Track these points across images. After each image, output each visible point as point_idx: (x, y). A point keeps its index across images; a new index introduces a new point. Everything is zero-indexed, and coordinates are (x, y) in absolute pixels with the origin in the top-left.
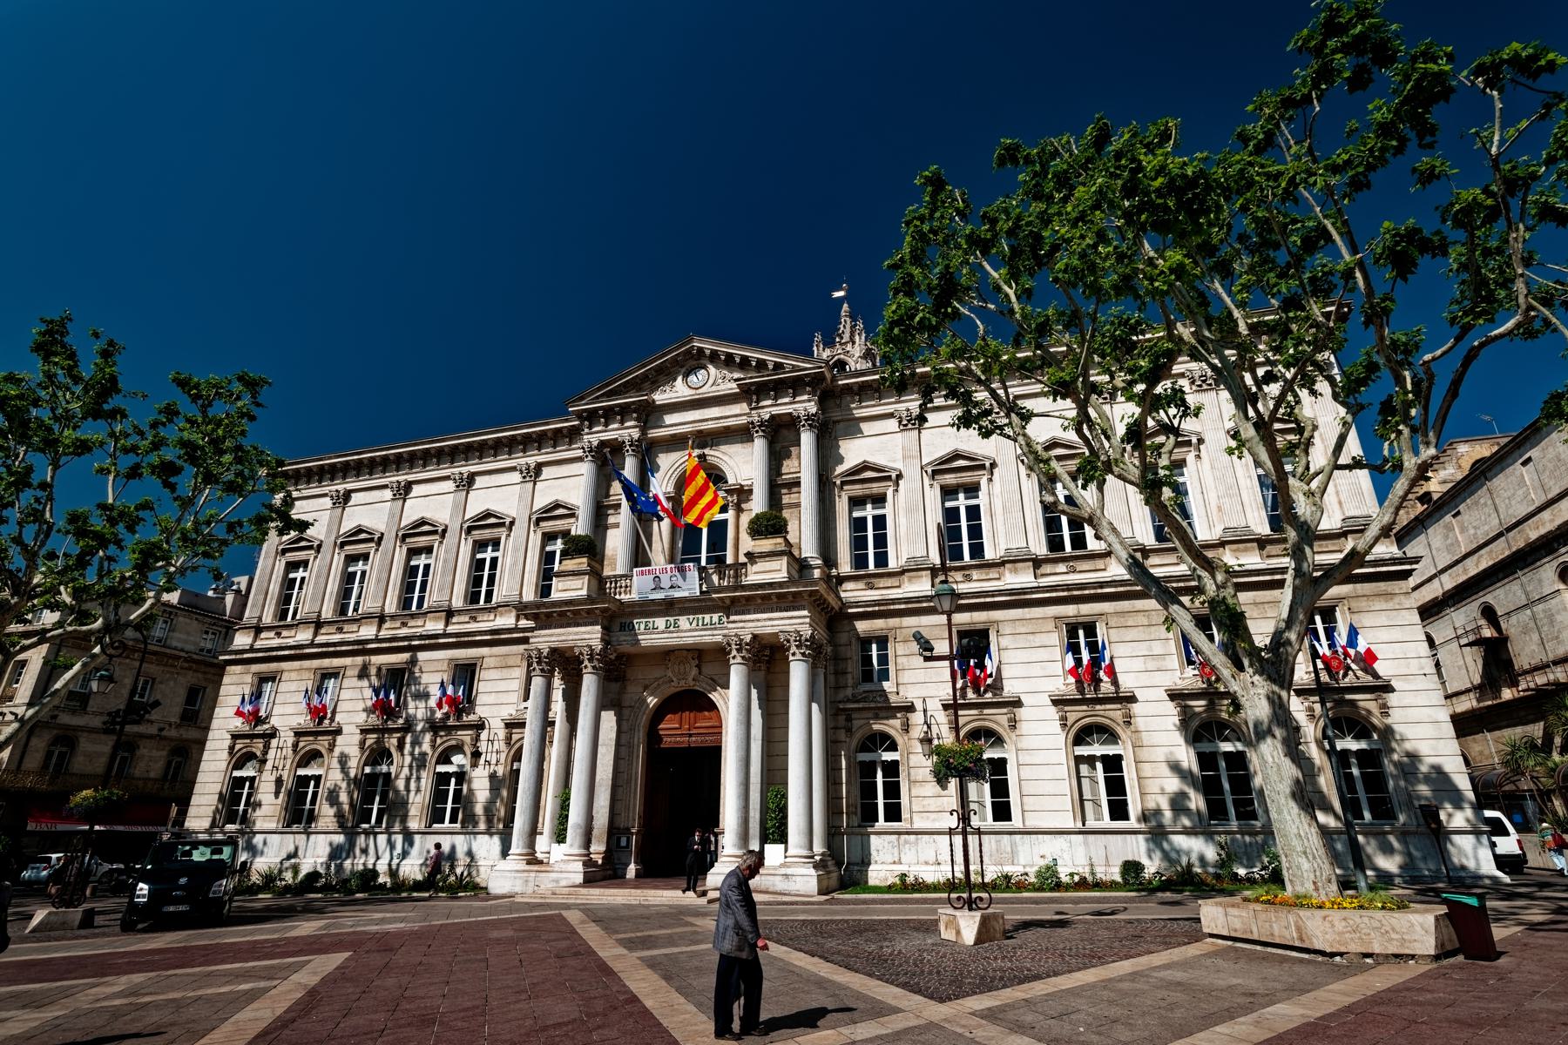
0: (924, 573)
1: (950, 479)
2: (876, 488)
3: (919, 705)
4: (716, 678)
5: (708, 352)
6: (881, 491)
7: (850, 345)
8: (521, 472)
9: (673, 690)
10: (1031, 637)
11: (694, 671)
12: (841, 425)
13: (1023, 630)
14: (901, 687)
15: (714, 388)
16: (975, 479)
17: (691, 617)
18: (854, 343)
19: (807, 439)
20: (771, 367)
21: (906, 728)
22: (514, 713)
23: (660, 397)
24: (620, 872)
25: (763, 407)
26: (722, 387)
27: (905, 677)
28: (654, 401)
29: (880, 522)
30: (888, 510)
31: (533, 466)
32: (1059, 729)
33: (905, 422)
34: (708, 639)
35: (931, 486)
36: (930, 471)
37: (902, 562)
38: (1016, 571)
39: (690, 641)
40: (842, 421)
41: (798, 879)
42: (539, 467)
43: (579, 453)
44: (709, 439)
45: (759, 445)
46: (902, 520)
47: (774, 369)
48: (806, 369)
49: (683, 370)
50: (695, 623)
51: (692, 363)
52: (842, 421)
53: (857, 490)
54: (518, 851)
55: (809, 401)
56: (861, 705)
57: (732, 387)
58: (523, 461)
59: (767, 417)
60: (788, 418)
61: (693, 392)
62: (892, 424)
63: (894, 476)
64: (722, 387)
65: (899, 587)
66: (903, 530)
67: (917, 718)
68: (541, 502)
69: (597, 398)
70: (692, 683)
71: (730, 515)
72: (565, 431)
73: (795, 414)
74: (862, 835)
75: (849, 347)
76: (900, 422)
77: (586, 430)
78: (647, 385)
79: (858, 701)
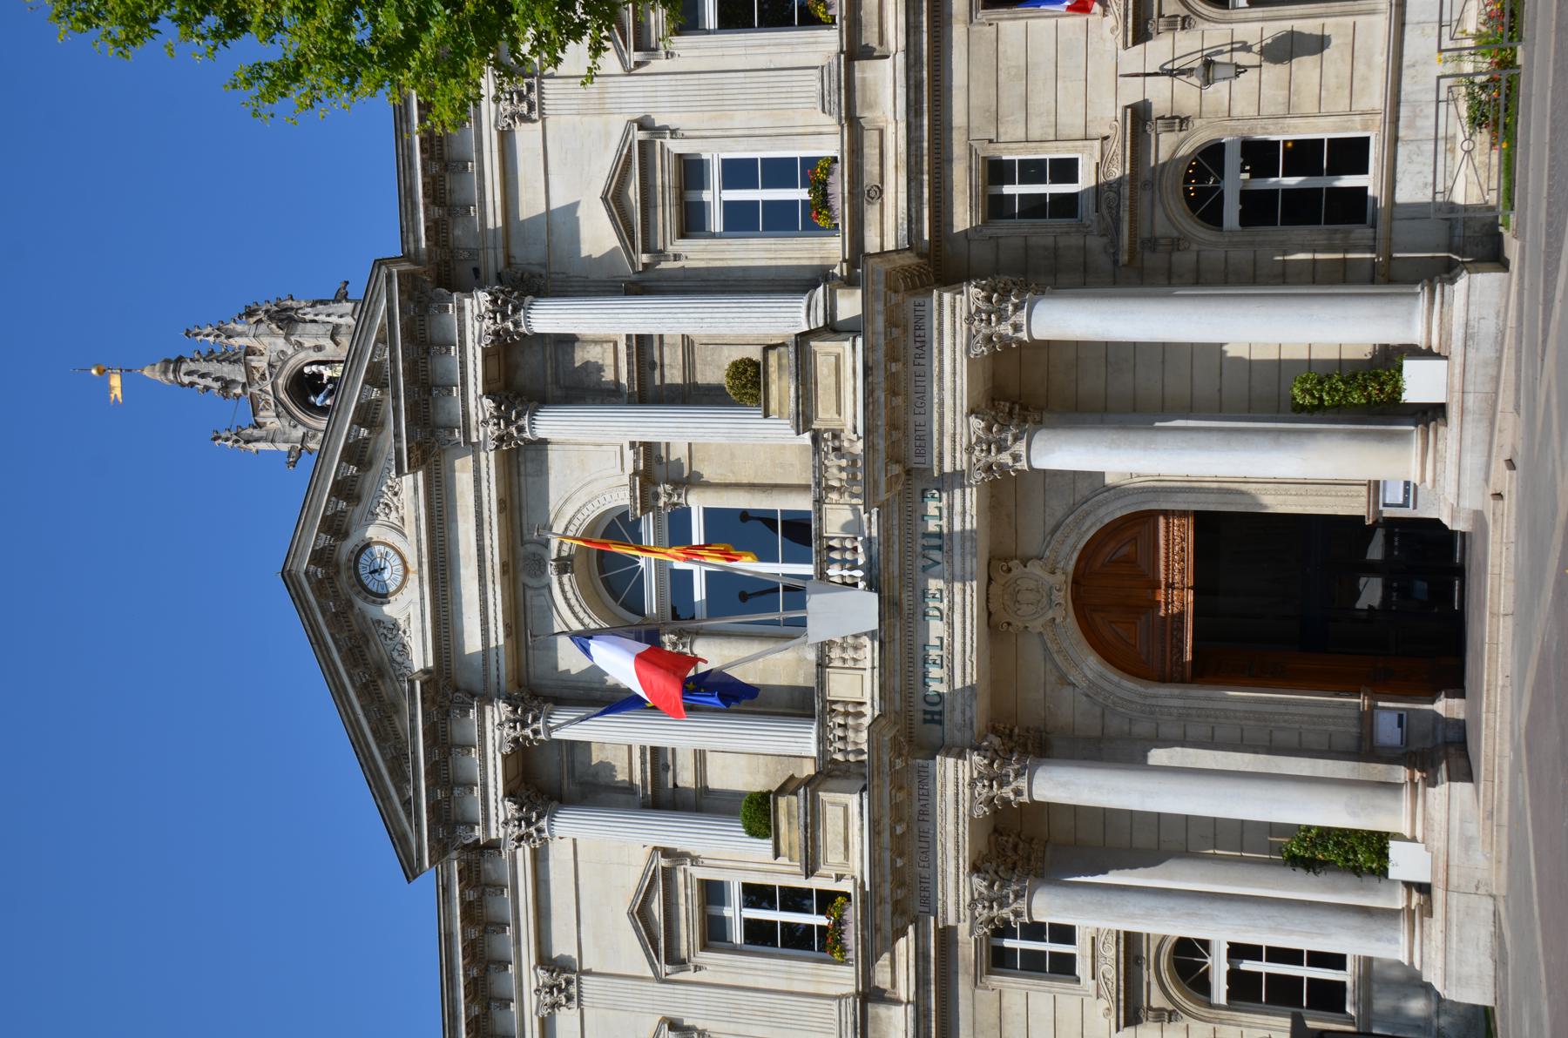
0: (858, 75)
2: (664, 177)
3: (1133, 92)
4: (1051, 522)
5: (325, 539)
6: (671, 166)
7: (256, 361)
8: (555, 1005)
9: (1072, 621)
11: (1035, 569)
12: (517, 251)
14: (1092, 132)
15: (409, 529)
17: (920, 562)
18: (250, 351)
19: (547, 318)
21: (1178, 122)
22: (1104, 1004)
23: (420, 655)
24: (1452, 735)
25: (466, 415)
26: (408, 512)
27: (1072, 122)
28: (425, 671)
29: (738, 173)
30: (714, 155)
31: (544, 976)
33: (524, 108)
35: (670, 55)
36: (637, 56)
37: (830, 123)
40: (507, 247)
41: (1474, 314)
42: (545, 960)
43: (524, 854)
44: (521, 551)
45: (549, 424)
46: (739, 120)
47: (382, 386)
48: (390, 310)
49: (359, 603)
50: (936, 555)
51: (344, 580)
52: (507, 247)
53: (666, 216)
54: (1403, 938)
55: (461, 309)
56: (1125, 216)
57: (408, 492)
58: (530, 1001)
59: (488, 403)
60: (493, 363)
61: (413, 578)
62: (527, 137)
63: (641, 135)
65: (881, 132)
66: (760, 121)
67: (1160, 94)
68: (629, 953)
69: (406, 803)
70: (1060, 577)
71: (697, 503)
72: (472, 895)
73: (487, 341)
74: (1392, 219)
75: (260, 363)
76: (525, 119)
77: (478, 832)
78: (385, 688)
79: (1117, 221)
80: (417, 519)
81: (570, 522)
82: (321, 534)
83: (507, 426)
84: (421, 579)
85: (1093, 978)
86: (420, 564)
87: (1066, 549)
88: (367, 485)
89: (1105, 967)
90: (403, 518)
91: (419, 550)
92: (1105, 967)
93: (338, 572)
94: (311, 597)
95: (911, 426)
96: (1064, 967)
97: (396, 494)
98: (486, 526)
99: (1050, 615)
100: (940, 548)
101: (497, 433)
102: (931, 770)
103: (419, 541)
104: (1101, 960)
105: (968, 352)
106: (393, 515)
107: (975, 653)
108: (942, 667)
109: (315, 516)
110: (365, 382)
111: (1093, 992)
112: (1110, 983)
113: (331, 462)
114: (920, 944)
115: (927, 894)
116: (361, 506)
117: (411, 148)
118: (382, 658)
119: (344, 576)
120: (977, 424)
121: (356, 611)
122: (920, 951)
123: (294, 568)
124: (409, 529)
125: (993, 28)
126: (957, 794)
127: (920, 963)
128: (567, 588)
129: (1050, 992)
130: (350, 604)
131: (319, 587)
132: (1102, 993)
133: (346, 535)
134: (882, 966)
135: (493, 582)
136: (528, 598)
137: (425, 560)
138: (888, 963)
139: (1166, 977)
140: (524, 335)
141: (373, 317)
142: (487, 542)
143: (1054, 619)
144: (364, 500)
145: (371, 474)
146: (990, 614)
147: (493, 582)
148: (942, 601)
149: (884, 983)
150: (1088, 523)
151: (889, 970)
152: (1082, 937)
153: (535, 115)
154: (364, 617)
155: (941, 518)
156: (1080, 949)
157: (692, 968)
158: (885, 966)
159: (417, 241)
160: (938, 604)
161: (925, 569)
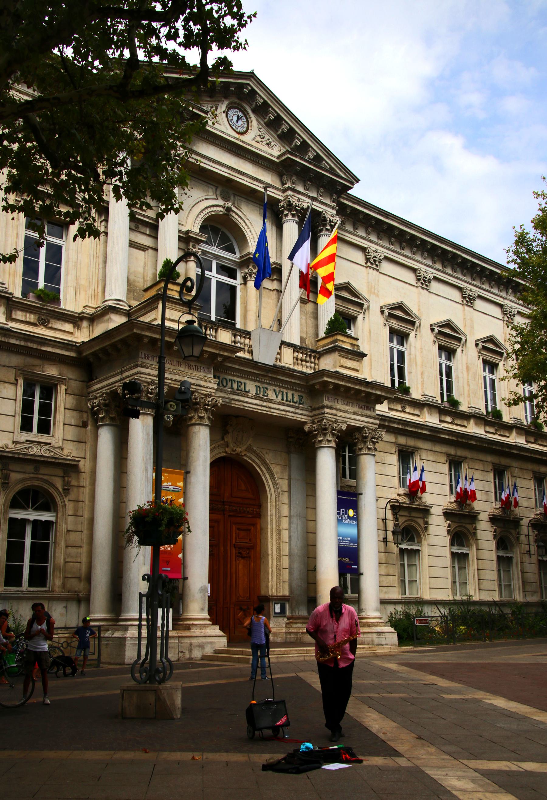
1: (395, 324)
10: (434, 464)
13: (431, 458)
16: (408, 331)
17: (277, 389)
20: (311, 155)
22: (11, 446)
25: (299, 192)
26: (259, 146)
32: (446, 534)
34: (290, 416)
38: (430, 413)
39: (276, 413)
49: (226, 103)
55: (333, 208)
61: (237, 136)
64: (259, 146)
80: (261, 150)
81: (244, 221)
82: (262, 101)
83: (296, 210)
84: (237, 139)
85: (27, 441)
86: (243, 142)
87: (254, 458)
88: (272, 133)
89: (35, 449)
90: (258, 142)
91: (249, 145)
92: (35, 449)
93: (239, 99)
94: (240, 81)
95: (337, 398)
96: (26, 426)
97: (268, 144)
98: (252, 181)
99: (231, 445)
100: (283, 399)
101: (294, 204)
102: (209, 376)
103: (252, 146)
104: (39, 447)
105: (367, 428)
106: (259, 139)
107: (243, 407)
108: (238, 390)
109: (272, 102)
110: (317, 153)
111: (17, 439)
112: (26, 450)
113: (292, 122)
114: (50, 343)
115: (150, 358)
116: (264, 125)
117: (370, 210)
118: (203, 101)
119: (237, 101)
120: (344, 427)
121: (223, 99)
122: (47, 342)
123: (253, 80)
124: (254, 143)
125: (394, 452)
126: (200, 386)
127: (39, 340)
128: (218, 209)
129: (15, 413)
130: (226, 97)
131: (241, 86)
132: (18, 445)
133: (254, 111)
134: (26, 316)
135: (229, 174)
136: (212, 186)
137: (244, 145)
138: (28, 320)
139: (28, 483)
140: (321, 230)
141: (340, 170)
142: (246, 179)
143: (228, 447)
144: (266, 128)
145: (276, 136)
146: (237, 417)
147: (229, 174)
148: (263, 395)
149: (15, 314)
150: (263, 469)
151: (24, 319)
152: (43, 438)
153: (369, 264)
154: (220, 101)
155: (293, 402)
156: (34, 435)
157: (17, 199)
158: (26, 318)
159: (344, 198)
160: (262, 393)
161: (275, 390)
